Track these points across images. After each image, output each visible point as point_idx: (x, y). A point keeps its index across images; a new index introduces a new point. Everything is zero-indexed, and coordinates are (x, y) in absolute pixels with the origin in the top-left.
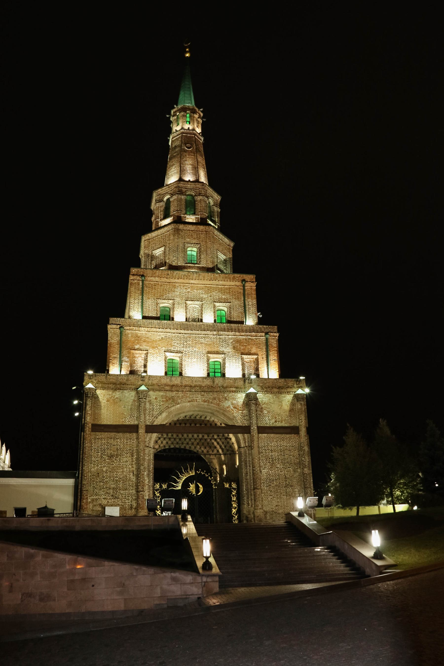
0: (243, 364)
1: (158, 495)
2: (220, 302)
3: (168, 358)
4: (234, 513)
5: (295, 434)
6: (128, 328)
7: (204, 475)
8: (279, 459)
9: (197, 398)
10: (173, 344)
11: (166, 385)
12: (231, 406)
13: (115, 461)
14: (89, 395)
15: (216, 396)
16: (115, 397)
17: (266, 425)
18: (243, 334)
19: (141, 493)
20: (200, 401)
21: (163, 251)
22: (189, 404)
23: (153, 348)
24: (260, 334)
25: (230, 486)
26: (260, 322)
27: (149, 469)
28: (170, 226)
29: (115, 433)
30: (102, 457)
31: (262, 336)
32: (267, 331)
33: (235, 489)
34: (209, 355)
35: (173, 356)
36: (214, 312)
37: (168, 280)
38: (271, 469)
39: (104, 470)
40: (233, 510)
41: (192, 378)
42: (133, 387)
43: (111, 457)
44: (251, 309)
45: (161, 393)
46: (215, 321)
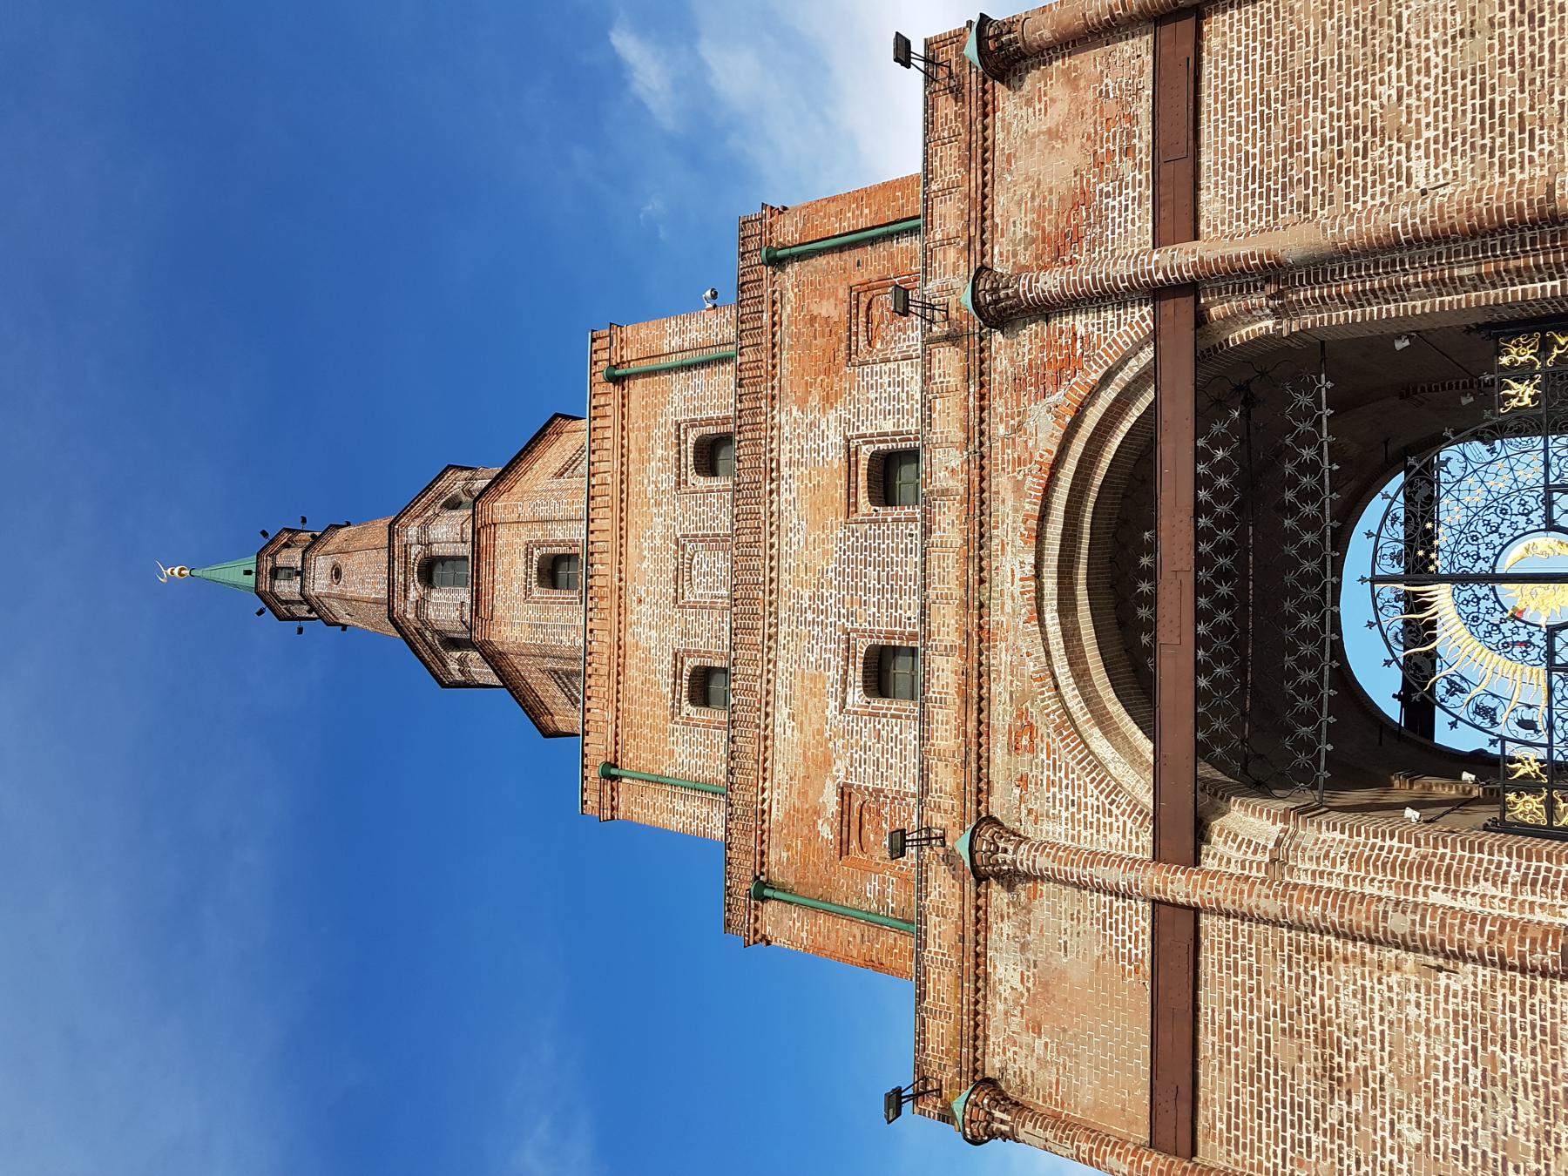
9: (1018, 576)
13: (1363, 1061)
16: (1020, 988)
25: (1522, 373)
27: (1409, 868)
30: (1333, 1132)
39: (1416, 1137)
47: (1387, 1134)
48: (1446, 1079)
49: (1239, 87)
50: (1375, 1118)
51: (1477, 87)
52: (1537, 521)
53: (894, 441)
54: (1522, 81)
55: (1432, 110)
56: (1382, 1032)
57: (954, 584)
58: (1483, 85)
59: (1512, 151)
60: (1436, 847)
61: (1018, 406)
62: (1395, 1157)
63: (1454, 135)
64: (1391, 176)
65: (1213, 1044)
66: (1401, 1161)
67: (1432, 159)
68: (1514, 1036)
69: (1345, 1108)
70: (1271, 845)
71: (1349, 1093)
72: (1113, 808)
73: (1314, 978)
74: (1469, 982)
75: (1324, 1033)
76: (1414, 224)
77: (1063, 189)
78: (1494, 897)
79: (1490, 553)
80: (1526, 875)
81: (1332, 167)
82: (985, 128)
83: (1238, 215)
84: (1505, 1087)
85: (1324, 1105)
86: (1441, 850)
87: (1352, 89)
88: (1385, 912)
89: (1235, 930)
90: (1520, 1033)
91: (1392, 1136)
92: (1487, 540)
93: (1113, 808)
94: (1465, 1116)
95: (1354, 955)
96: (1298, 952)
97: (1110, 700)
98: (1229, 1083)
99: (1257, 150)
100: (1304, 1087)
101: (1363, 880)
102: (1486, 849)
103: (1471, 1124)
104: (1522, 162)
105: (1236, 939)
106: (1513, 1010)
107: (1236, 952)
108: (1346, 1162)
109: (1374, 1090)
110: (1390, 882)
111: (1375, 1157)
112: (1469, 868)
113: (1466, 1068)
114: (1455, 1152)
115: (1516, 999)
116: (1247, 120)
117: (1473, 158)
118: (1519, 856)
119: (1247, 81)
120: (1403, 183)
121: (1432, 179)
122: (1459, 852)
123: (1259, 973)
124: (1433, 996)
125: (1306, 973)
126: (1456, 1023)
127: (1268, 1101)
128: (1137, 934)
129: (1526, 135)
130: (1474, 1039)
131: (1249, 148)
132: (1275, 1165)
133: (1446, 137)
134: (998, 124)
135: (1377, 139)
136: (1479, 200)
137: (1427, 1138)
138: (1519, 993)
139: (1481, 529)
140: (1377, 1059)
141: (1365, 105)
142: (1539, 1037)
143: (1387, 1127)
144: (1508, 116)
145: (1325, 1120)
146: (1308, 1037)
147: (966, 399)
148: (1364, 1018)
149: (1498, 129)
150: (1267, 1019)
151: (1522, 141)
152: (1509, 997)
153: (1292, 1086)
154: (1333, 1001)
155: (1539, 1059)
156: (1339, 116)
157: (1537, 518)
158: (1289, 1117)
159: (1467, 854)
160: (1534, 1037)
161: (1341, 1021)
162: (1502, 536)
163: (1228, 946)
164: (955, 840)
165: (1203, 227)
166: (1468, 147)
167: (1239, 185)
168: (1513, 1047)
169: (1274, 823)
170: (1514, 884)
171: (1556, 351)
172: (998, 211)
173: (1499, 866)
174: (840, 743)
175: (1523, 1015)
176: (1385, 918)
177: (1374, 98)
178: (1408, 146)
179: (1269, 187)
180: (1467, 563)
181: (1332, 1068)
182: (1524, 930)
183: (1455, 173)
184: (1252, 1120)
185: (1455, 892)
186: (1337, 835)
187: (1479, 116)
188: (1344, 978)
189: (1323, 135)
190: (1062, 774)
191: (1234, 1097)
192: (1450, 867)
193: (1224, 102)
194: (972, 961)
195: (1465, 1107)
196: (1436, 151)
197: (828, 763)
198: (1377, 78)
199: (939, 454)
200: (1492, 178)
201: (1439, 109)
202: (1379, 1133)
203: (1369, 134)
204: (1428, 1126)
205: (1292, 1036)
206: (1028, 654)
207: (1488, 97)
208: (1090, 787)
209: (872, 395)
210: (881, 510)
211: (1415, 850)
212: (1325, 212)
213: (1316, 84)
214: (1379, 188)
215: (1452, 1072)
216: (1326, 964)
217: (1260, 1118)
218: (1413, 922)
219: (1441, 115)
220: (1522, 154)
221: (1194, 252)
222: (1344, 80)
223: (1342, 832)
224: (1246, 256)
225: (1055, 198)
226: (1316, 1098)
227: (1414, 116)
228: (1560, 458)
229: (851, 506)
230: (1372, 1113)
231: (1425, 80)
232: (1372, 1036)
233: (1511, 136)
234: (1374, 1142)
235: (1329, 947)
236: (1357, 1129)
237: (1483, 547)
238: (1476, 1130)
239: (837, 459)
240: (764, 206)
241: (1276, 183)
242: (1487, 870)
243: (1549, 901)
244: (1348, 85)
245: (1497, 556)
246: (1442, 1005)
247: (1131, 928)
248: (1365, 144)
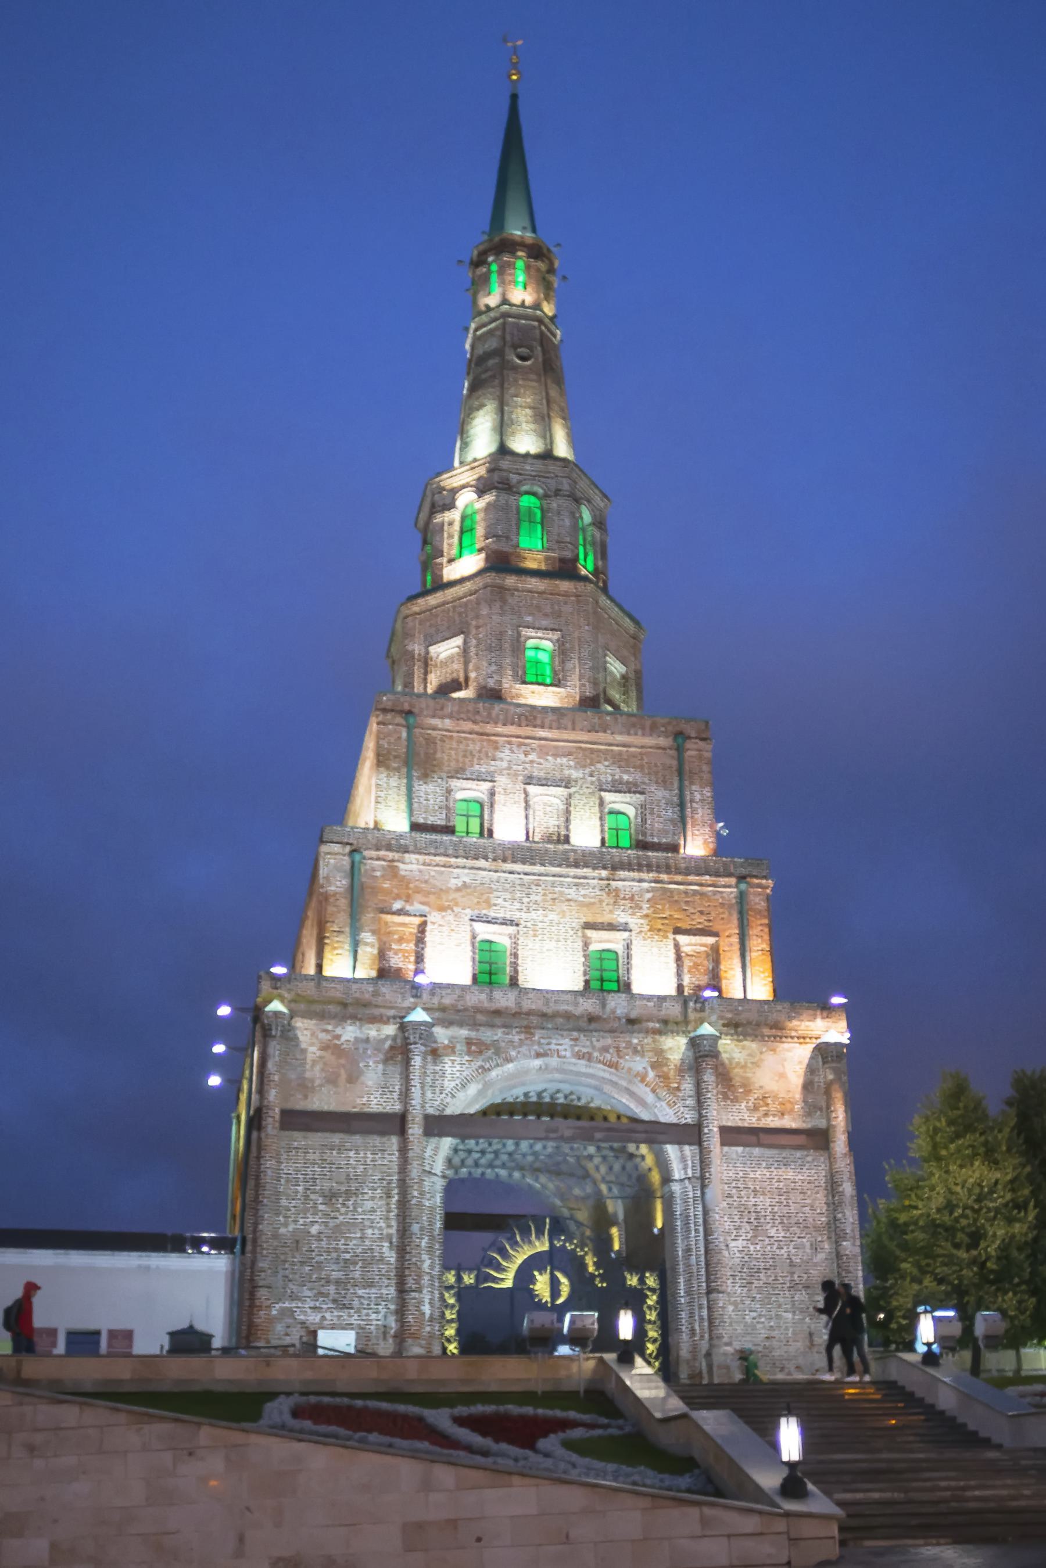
0: (679, 959)
2: (616, 792)
3: (479, 939)
4: (650, 1355)
5: (816, 1148)
6: (373, 853)
7: (574, 1250)
10: (494, 901)
11: (478, 1010)
14: (273, 1033)
18: (679, 878)
19: (413, 1294)
20: (568, 1054)
21: (458, 647)
23: (442, 909)
24: (723, 881)
25: (642, 1280)
26: (722, 847)
28: (477, 579)
29: (342, 1135)
30: (307, 1197)
31: (729, 886)
32: (743, 871)
33: (653, 1290)
34: (589, 933)
35: (494, 933)
36: (601, 819)
37: (476, 728)
38: (753, 1240)
39: (314, 1230)
41: (547, 992)
42: (392, 1013)
43: (330, 1197)
44: (700, 811)
45: (464, 1032)
46: (603, 841)
82: (792, 1038)
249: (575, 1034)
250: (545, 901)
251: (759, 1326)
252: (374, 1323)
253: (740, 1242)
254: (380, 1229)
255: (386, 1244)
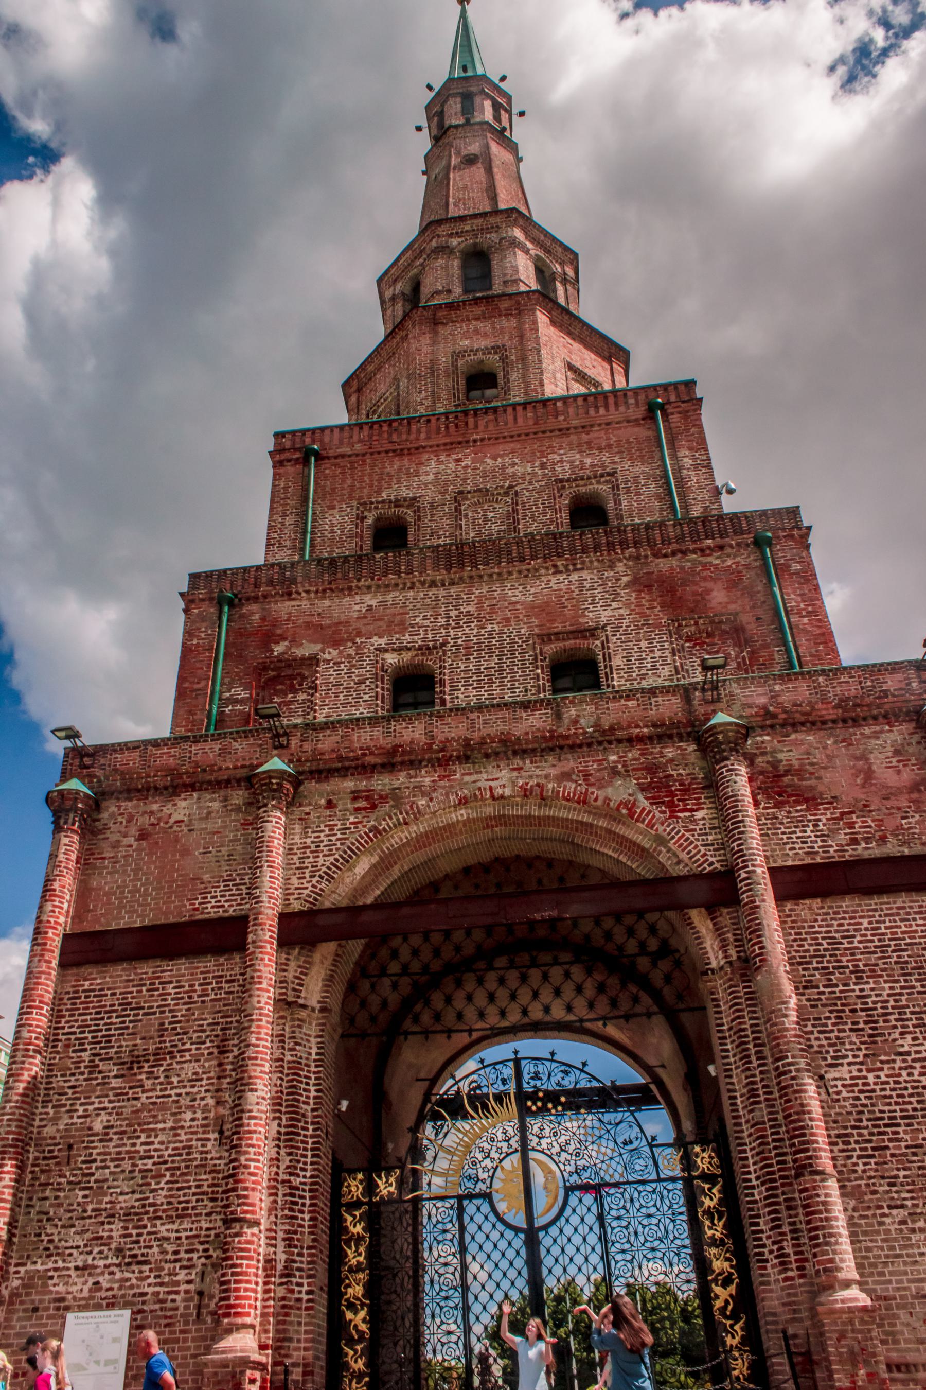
1: (358, 1229)
4: (723, 1310)
8: (901, 1009)
12: (640, 797)
13: (148, 1084)
15: (572, 764)
16: (172, 821)
17: (808, 861)
22: (463, 813)
30: (93, 1067)
39: (98, 1126)
40: (718, 1289)
43: (131, 1064)
47: (96, 1105)
48: (142, 1144)
49: (911, 926)
50: (107, 1096)
51: (911, 1113)
52: (572, 1180)
53: (606, 667)
54: (916, 1146)
55: (890, 1080)
56: (170, 1096)
57: (484, 732)
58: (913, 1117)
59: (857, 1142)
60: (313, 1123)
61: (634, 770)
62: (81, 1113)
63: (870, 1098)
64: (835, 1051)
65: (146, 973)
66: (79, 1117)
67: (849, 1082)
68: (179, 1189)
69: (112, 1074)
70: (301, 1001)
71: (122, 1076)
72: (317, 878)
73: (204, 1043)
74: (214, 1154)
75: (164, 1054)
76: (790, 1071)
77: (821, 788)
78: (278, 1167)
79: (544, 1146)
80: (298, 1189)
81: (842, 1005)
82: (875, 718)
83: (800, 934)
84: (141, 1185)
85: (111, 1059)
86: (311, 1127)
87: (909, 1016)
88: (256, 1090)
89: (233, 981)
90: (181, 1193)
91: (95, 1109)
92: (555, 1144)
93: (317, 878)
94: (117, 1159)
95: (225, 1070)
96: (222, 1029)
97: (402, 866)
98: (119, 988)
99: (856, 944)
100: (124, 1043)
101: (281, 1072)
102: (315, 1159)
103: (112, 1164)
104: (847, 1150)
105: (227, 982)
106: (197, 1187)
107: (217, 983)
108: (73, 1078)
109: (127, 1094)
110: (282, 1092)
111: (79, 1099)
112: (299, 1148)
113: (152, 1157)
114: (91, 1154)
115: (205, 1188)
116: (883, 934)
117: (850, 1113)
118: (312, 1184)
119: (916, 932)
120: (829, 1061)
121: (832, 1083)
122: (310, 1141)
123: (203, 1002)
124: (200, 1130)
125: (207, 1037)
126: (184, 1148)
127: (109, 1018)
128: (223, 906)
129: (870, 1152)
130: (173, 1162)
131: (859, 938)
132: (63, 1028)
133: (868, 1091)
134: (878, 728)
135: (866, 1039)
136: (811, 1119)
137: (97, 1134)
138: (210, 1190)
139: (562, 1139)
140: (150, 1094)
141: (895, 1027)
142: (180, 1206)
143: (102, 1106)
144: (886, 1137)
145: (101, 1060)
146: (160, 1042)
147: (637, 726)
148: (179, 1082)
149: (875, 1130)
150: (170, 1011)
151: (866, 1149)
152: (206, 1183)
153: (122, 1034)
154: (188, 1058)
155: (165, 1207)
156: (887, 1008)
157: (574, 1179)
158: (100, 1034)
159: (309, 1146)
160: (180, 1203)
161: (175, 1066)
162: (558, 1154)
163: (221, 976)
164: (279, 756)
165: (789, 906)
166: (860, 1108)
167: (827, 932)
168: (170, 1189)
169: (319, 1002)
170: (289, 1181)
171: (707, 1186)
172: (800, 736)
173: (303, 1169)
174: (352, 652)
175: (194, 1194)
176: (251, 1090)
177: (902, 1034)
178: (861, 1063)
179: (824, 956)
180: (536, 1129)
181: (139, 1062)
182: (253, 1189)
183: (838, 1100)
184: (94, 1007)
185: (279, 1139)
186: (314, 1051)
187: (886, 1115)
188: (207, 1064)
189: (869, 996)
190: (339, 836)
191: (109, 992)
192: (299, 1134)
193: (898, 914)
194: (188, 781)
195: (123, 1159)
196: (856, 1085)
197: (336, 643)
198: (918, 1035)
199: (590, 709)
200: (834, 1129)
201: (892, 1085)
202: (97, 1100)
203: (871, 1032)
204: (107, 1134)
205: (159, 1030)
206: (431, 800)
207: (902, 1122)
208: (331, 859)
209: (644, 644)
210: (547, 662)
211: (309, 1108)
212: (805, 1002)
213: (913, 987)
214: (825, 1042)
215: (147, 1147)
216: (215, 1051)
217: (97, 1013)
218: (251, 1111)
219: (887, 1087)
220: (854, 1150)
221: (764, 901)
222: (917, 1009)
223: (317, 1054)
224: (761, 942)
225: (813, 782)
226: (116, 1053)
227: (886, 1066)
228: (622, 1194)
229: (546, 638)
230: (111, 1093)
231: (916, 1072)
232: (166, 1089)
233: (870, 1141)
234: (89, 1097)
235: (228, 1051)
236: (98, 1084)
237: (549, 1140)
238: (108, 1167)
239: (589, 619)
240: (809, 528)
241: (828, 962)
242: (299, 1161)
243: (279, 1206)
244: (912, 1013)
245: (542, 1152)
246: (195, 1137)
247: (226, 901)
248: (862, 1030)
249: (517, 762)
250: (480, 609)
251: (914, 1238)
252: (183, 1287)
253: (846, 1068)
254: (205, 1109)
255: (213, 1136)
